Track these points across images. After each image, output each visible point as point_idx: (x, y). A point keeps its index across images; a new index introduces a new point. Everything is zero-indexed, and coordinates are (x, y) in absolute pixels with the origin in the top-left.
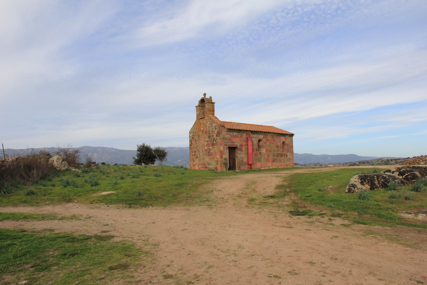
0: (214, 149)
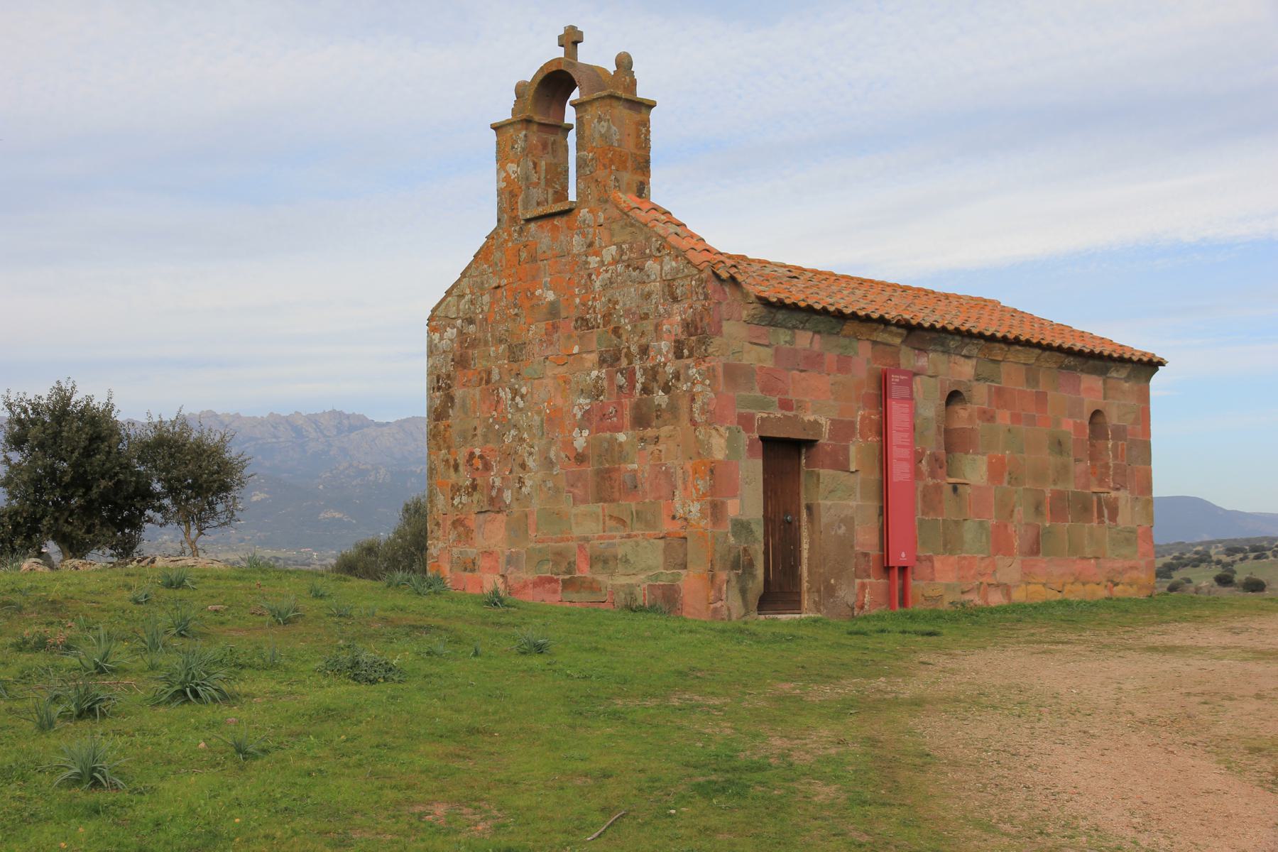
0: (651, 448)
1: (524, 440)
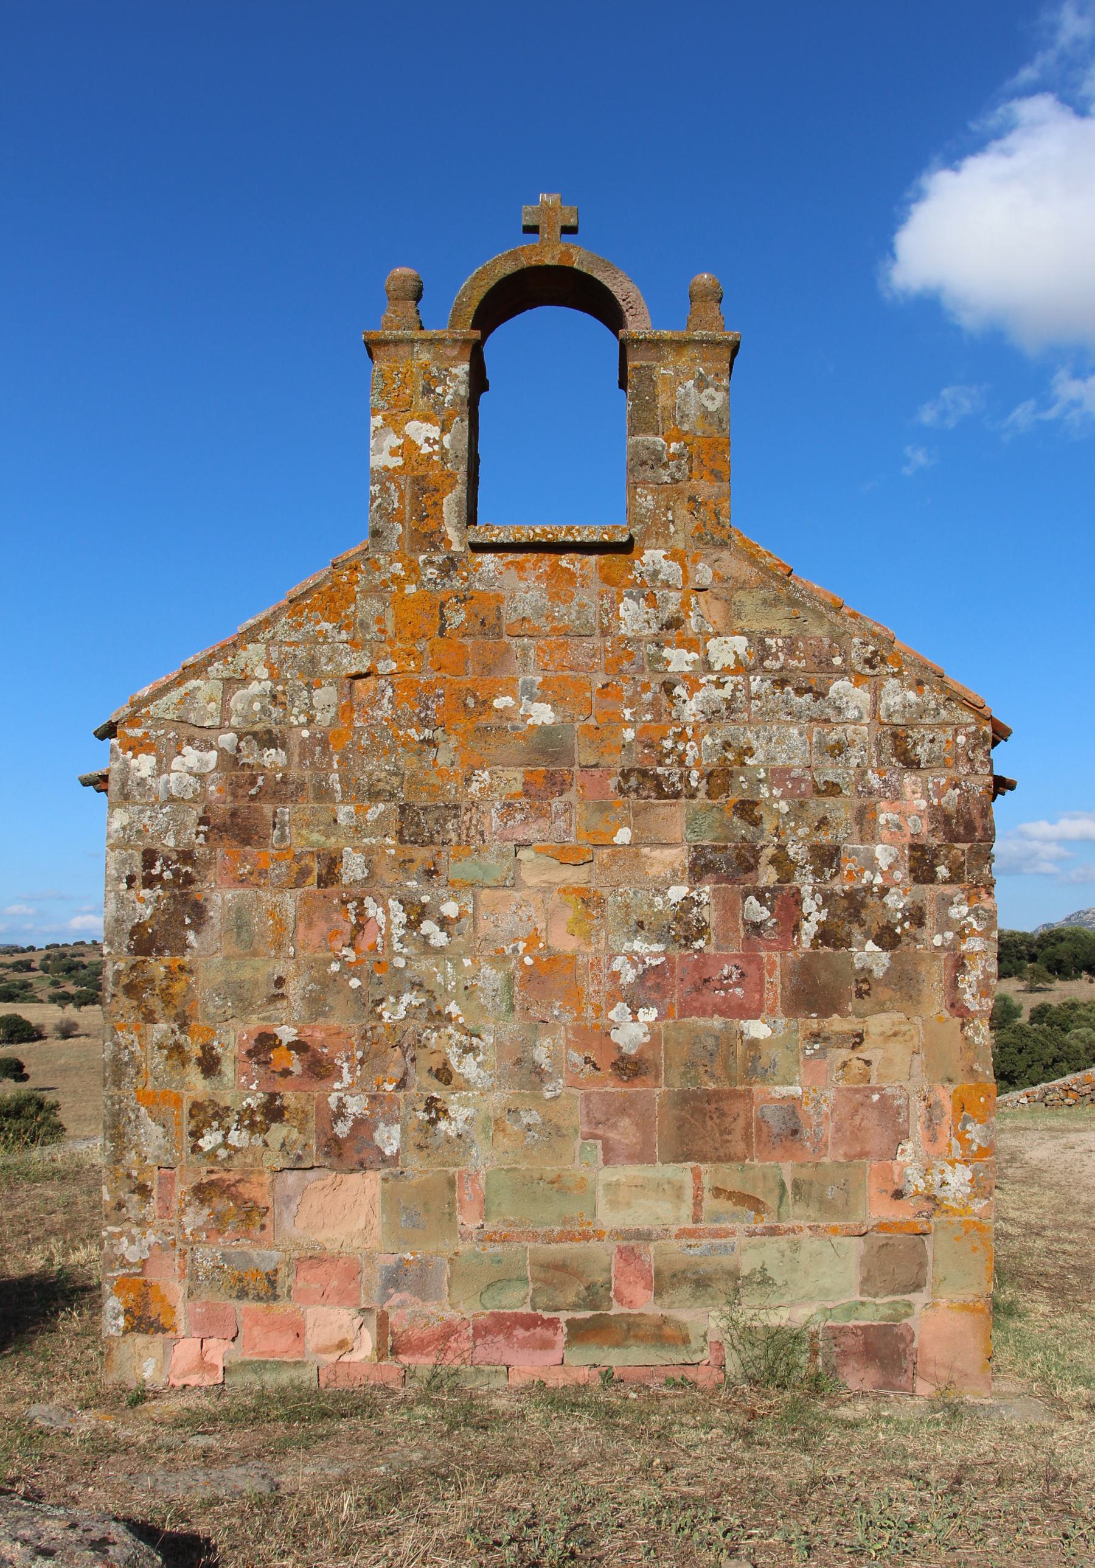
1: (449, 1018)
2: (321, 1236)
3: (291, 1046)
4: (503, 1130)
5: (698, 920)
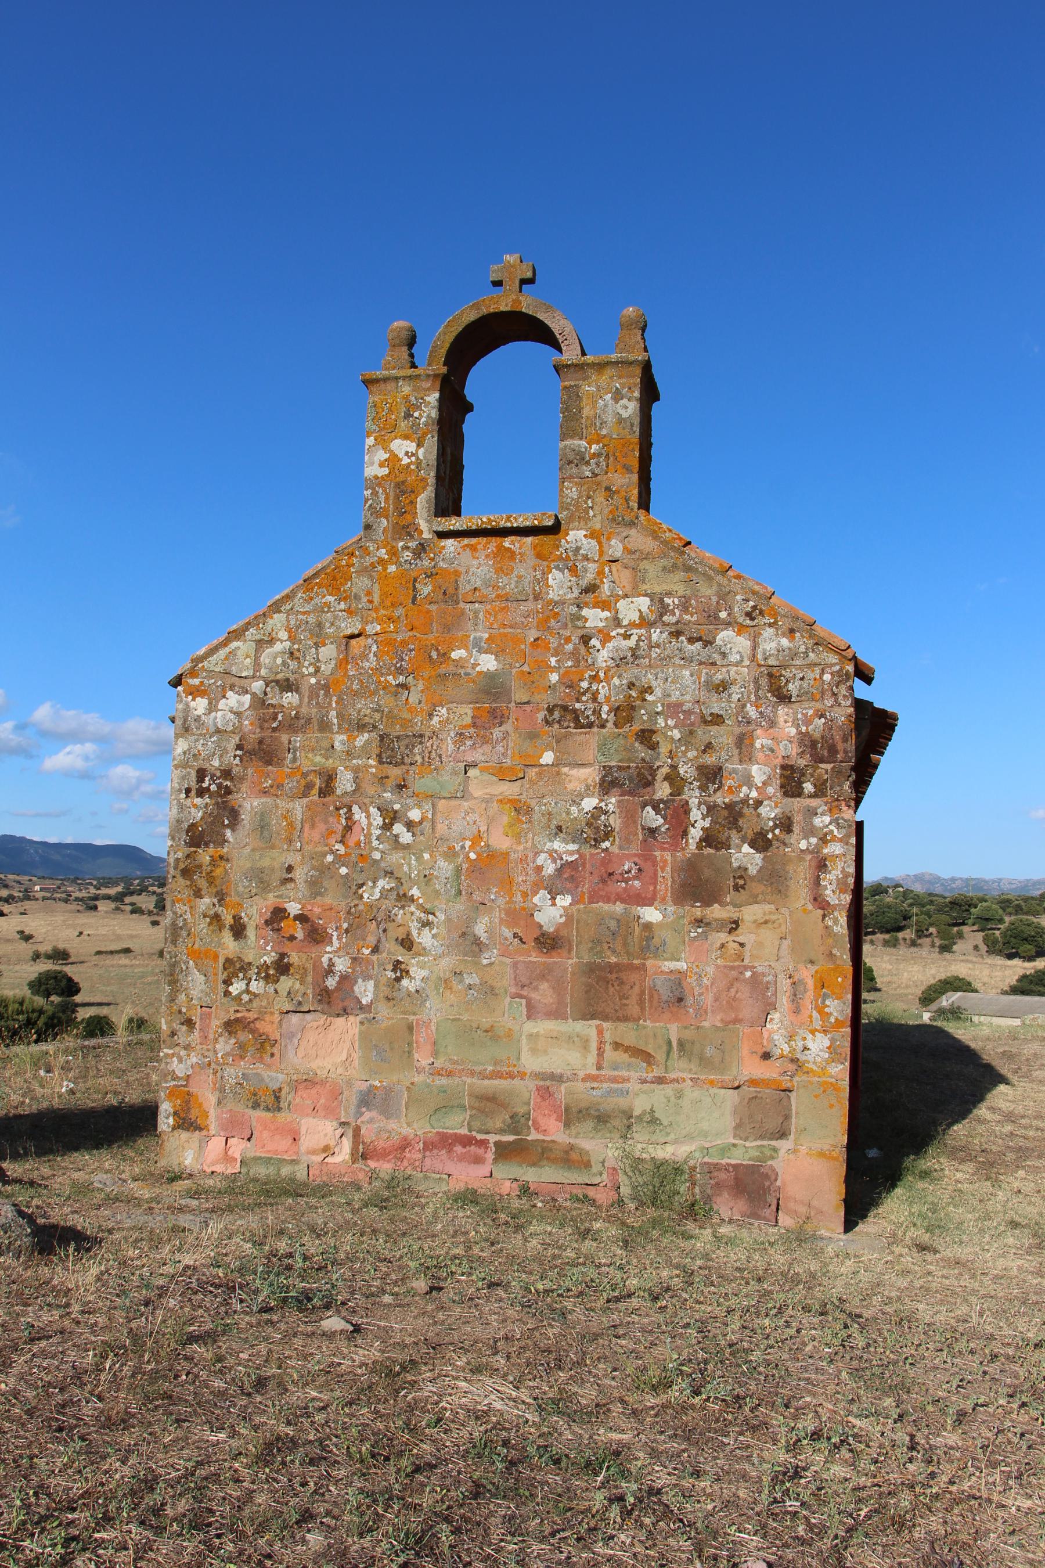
1: (412, 899)
2: (314, 1065)
3: (297, 918)
4: (451, 988)
5: (605, 826)
